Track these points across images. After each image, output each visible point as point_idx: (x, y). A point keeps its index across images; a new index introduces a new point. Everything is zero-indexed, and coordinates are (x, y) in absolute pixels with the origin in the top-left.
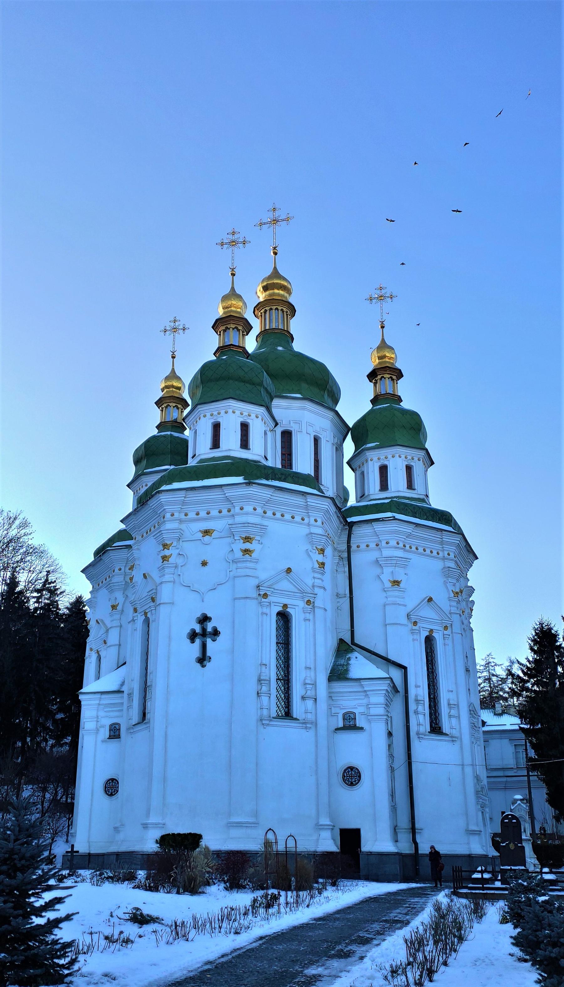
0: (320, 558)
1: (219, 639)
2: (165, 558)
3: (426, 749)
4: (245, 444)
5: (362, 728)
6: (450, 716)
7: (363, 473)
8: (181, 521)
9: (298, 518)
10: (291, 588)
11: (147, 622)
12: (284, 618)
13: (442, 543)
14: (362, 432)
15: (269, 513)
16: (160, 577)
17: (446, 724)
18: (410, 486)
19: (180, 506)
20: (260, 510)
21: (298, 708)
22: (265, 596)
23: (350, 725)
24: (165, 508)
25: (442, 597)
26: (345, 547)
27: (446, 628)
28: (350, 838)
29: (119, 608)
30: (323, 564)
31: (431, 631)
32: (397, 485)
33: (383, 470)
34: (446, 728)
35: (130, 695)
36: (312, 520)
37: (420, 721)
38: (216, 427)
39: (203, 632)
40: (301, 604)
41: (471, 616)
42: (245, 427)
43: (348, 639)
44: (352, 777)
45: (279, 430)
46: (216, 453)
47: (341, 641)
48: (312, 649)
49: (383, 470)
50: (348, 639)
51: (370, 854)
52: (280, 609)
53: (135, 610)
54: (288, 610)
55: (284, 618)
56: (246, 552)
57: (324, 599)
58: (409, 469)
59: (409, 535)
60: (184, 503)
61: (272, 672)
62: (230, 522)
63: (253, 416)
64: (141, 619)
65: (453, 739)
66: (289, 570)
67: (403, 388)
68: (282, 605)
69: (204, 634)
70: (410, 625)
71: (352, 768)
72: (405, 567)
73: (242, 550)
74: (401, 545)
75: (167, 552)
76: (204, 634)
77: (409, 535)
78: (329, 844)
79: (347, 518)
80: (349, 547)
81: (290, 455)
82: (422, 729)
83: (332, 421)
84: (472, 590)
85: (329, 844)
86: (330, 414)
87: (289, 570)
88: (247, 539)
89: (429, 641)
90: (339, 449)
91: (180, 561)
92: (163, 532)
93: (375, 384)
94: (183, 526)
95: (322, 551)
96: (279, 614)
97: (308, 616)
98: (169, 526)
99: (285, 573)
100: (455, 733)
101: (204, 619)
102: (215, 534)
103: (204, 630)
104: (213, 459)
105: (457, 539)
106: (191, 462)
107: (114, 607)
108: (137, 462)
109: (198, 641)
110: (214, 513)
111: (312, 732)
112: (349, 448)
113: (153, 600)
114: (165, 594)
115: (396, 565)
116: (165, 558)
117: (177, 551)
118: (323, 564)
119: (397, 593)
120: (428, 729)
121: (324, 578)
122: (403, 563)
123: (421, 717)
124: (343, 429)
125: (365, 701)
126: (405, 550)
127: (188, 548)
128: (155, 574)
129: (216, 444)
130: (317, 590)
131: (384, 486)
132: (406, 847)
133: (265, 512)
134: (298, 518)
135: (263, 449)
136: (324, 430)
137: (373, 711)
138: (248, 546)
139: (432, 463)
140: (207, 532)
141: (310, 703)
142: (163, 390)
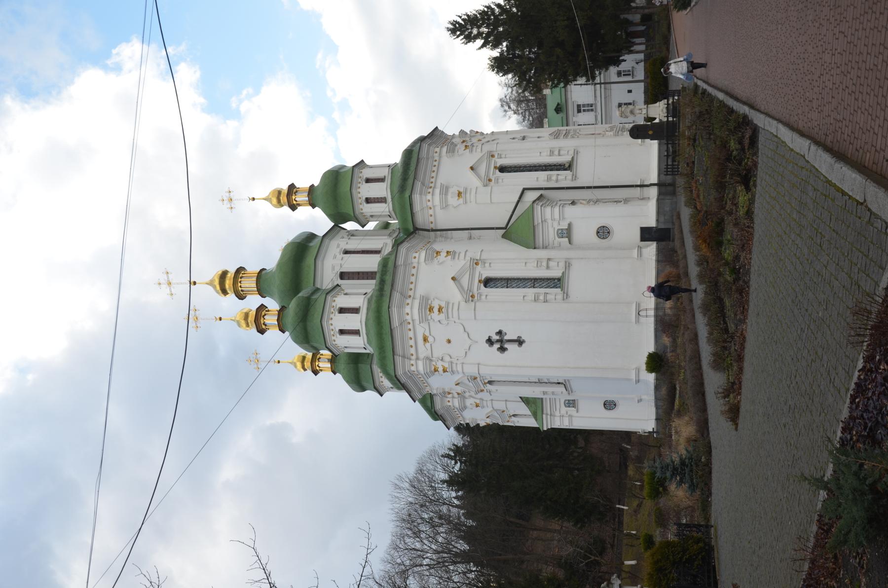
0: (444, 254)
1: (504, 331)
2: (445, 371)
3: (585, 174)
4: (356, 311)
5: (570, 225)
6: (559, 155)
7: (372, 216)
9: (414, 271)
10: (467, 276)
11: (490, 382)
12: (488, 282)
13: (428, 158)
14: (338, 217)
17: (565, 159)
18: (382, 180)
20: (409, 301)
21: (556, 273)
22: (473, 296)
23: (567, 233)
25: (471, 158)
26: (432, 233)
27: (493, 156)
28: (646, 234)
29: (478, 401)
30: (448, 252)
31: (495, 167)
32: (380, 190)
33: (368, 201)
34: (569, 158)
35: (544, 393)
36: (414, 260)
37: (563, 178)
38: (342, 332)
39: (500, 342)
41: (482, 134)
42: (342, 311)
43: (503, 231)
44: (603, 232)
45: (340, 282)
46: (363, 332)
47: (504, 236)
48: (510, 260)
49: (368, 201)
50: (503, 231)
51: (657, 220)
53: (482, 391)
55: (488, 282)
56: (440, 310)
57: (474, 250)
58: (368, 181)
59: (423, 184)
60: (404, 357)
62: (417, 322)
63: (334, 304)
64: (489, 387)
65: (576, 152)
67: (303, 183)
69: (501, 341)
70: (492, 183)
71: (598, 232)
72: (447, 188)
74: (430, 190)
75: (440, 369)
76: (501, 341)
77: (423, 184)
78: (651, 249)
79: (410, 230)
80: (433, 230)
81: (358, 273)
82: (570, 177)
83: (331, 240)
84: (462, 132)
85: (651, 249)
86: (326, 241)
87: (453, 279)
88: (431, 309)
89: (503, 169)
90: (352, 234)
91: (447, 359)
93: (299, 205)
94: (421, 356)
95: (438, 253)
96: (485, 286)
97: (487, 265)
98: (421, 368)
100: (571, 152)
101: (490, 341)
102: (427, 334)
103: (498, 341)
104: (367, 334)
105: (425, 146)
106: (370, 350)
107: (477, 406)
108: (362, 389)
109: (506, 346)
110: (411, 334)
111: (573, 262)
112: (350, 226)
113: (475, 378)
114: (472, 370)
115: (446, 194)
116: (445, 371)
118: (448, 252)
119: (468, 195)
120: (568, 172)
121: (458, 251)
122: (445, 190)
123: (560, 177)
124: (336, 229)
125: (550, 221)
126: (435, 187)
127: (437, 353)
128: (456, 378)
129: (356, 332)
130: (468, 258)
131: (382, 200)
132: (654, 192)
134: (414, 271)
135: (358, 295)
136: (338, 246)
137: (557, 216)
138: (436, 310)
139: (362, 161)
140: (425, 340)
141: (551, 264)
142: (305, 370)
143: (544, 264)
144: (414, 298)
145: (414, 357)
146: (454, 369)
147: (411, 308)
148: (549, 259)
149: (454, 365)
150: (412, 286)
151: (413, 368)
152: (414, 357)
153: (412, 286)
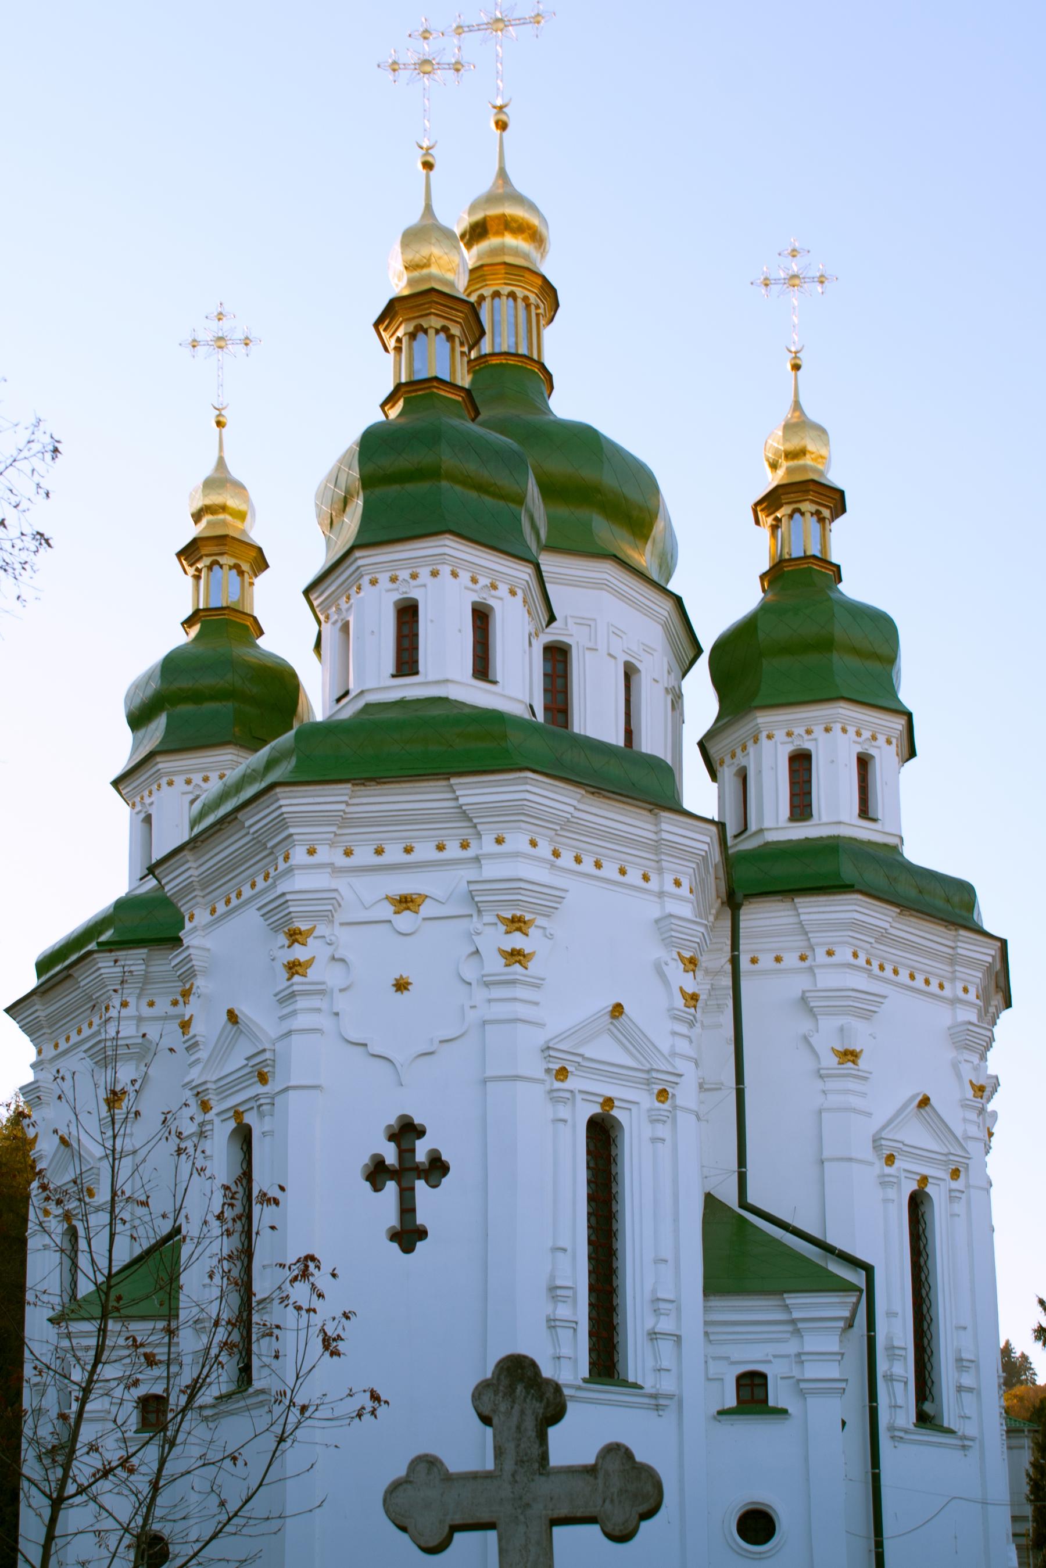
8: (336, 871)
10: (621, 1058)
15: (567, 859)
16: (282, 1018)
19: (334, 829)
24: (292, 830)
40: (646, 1100)
52: (597, 1109)
54: (614, 1112)
60: (345, 821)
61: (576, 1273)
66: (618, 1010)
68: (601, 1100)
73: (503, 953)
75: (299, 953)
92: (288, 897)
98: (301, 882)
99: (607, 1018)
101: (406, 1132)
113: (263, 1078)
116: (294, 968)
117: (329, 951)
133: (556, 854)
143: (666, 1325)
144: (553, 866)
145: (342, 861)
146: (301, 1003)
147: (516, 855)
148: (678, 1339)
149: (315, 1002)
150: (588, 865)
151: (299, 855)
152: (342, 861)
153: (588, 865)
